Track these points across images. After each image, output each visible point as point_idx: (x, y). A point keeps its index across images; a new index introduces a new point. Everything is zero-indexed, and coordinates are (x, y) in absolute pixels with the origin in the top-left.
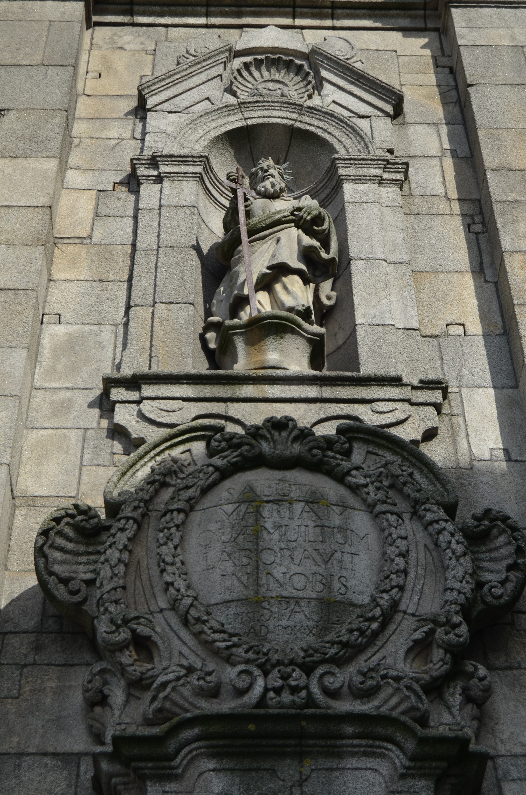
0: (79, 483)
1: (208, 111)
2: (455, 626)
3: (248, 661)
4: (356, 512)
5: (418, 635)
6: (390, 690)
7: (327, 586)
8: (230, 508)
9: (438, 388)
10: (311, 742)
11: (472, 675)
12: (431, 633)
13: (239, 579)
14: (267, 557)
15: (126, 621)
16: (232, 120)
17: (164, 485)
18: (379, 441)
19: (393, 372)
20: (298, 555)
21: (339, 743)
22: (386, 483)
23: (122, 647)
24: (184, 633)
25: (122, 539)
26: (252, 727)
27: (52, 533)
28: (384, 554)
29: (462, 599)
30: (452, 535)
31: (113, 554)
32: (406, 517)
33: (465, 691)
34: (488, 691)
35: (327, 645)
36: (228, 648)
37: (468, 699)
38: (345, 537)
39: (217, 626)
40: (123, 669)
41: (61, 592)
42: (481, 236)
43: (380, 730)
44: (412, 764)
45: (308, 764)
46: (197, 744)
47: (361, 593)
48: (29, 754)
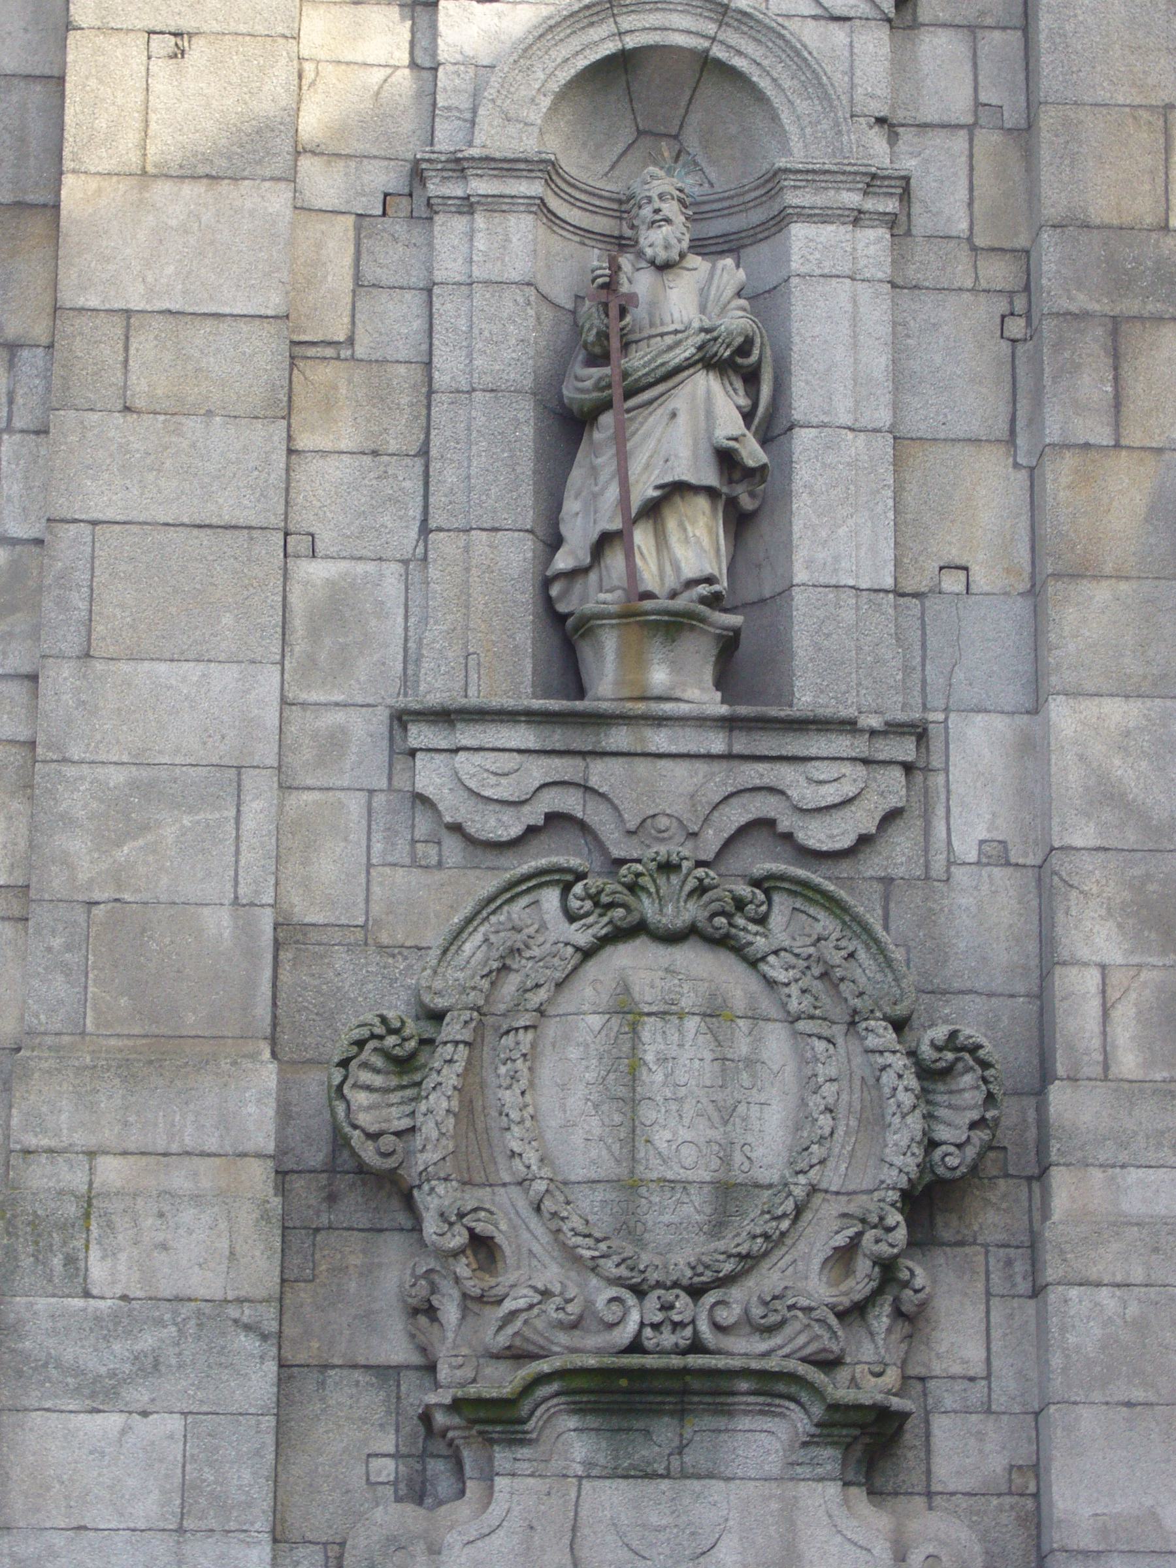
0: (367, 901)
1: (552, 22)
2: (889, 1230)
3: (618, 1281)
4: (770, 1026)
5: (840, 1240)
6: (797, 1326)
7: (726, 1161)
8: (595, 1021)
9: (911, 734)
10: (696, 1399)
11: (906, 1284)
12: (860, 1234)
13: (609, 1148)
14: (648, 1113)
15: (461, 1216)
16: (596, 38)
17: (505, 968)
18: (810, 894)
19: (845, 713)
20: (689, 1109)
21: (730, 1400)
22: (816, 971)
23: (456, 1254)
24: (534, 1222)
25: (450, 1077)
26: (624, 1383)
27: (354, 1063)
28: (803, 1103)
29: (903, 1182)
30: (900, 1076)
31: (439, 1102)
32: (838, 1031)
33: (897, 1301)
34: (923, 1305)
35: (722, 1257)
36: (593, 1258)
37: (899, 1314)
38: (753, 1076)
39: (581, 1227)
40: (457, 1280)
41: (368, 1153)
42: (1021, 349)
43: (781, 1387)
44: (818, 1431)
45: (693, 1425)
46: (555, 1401)
47: (771, 1166)
48: (334, 1367)
